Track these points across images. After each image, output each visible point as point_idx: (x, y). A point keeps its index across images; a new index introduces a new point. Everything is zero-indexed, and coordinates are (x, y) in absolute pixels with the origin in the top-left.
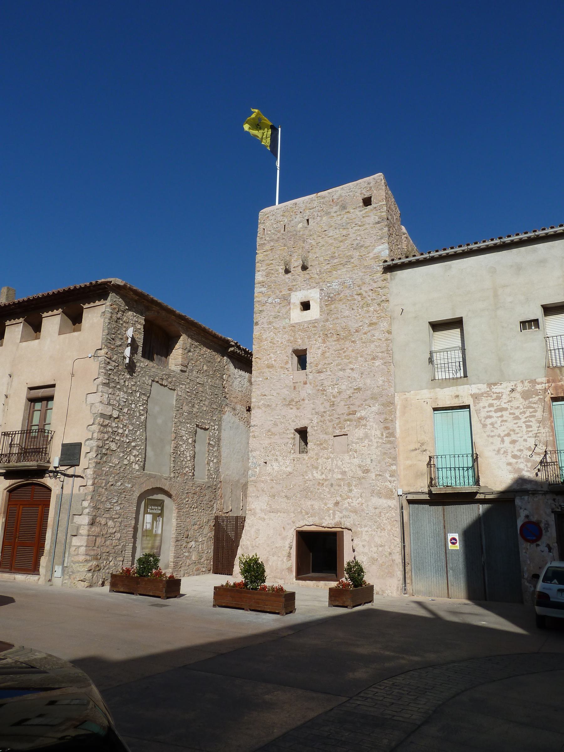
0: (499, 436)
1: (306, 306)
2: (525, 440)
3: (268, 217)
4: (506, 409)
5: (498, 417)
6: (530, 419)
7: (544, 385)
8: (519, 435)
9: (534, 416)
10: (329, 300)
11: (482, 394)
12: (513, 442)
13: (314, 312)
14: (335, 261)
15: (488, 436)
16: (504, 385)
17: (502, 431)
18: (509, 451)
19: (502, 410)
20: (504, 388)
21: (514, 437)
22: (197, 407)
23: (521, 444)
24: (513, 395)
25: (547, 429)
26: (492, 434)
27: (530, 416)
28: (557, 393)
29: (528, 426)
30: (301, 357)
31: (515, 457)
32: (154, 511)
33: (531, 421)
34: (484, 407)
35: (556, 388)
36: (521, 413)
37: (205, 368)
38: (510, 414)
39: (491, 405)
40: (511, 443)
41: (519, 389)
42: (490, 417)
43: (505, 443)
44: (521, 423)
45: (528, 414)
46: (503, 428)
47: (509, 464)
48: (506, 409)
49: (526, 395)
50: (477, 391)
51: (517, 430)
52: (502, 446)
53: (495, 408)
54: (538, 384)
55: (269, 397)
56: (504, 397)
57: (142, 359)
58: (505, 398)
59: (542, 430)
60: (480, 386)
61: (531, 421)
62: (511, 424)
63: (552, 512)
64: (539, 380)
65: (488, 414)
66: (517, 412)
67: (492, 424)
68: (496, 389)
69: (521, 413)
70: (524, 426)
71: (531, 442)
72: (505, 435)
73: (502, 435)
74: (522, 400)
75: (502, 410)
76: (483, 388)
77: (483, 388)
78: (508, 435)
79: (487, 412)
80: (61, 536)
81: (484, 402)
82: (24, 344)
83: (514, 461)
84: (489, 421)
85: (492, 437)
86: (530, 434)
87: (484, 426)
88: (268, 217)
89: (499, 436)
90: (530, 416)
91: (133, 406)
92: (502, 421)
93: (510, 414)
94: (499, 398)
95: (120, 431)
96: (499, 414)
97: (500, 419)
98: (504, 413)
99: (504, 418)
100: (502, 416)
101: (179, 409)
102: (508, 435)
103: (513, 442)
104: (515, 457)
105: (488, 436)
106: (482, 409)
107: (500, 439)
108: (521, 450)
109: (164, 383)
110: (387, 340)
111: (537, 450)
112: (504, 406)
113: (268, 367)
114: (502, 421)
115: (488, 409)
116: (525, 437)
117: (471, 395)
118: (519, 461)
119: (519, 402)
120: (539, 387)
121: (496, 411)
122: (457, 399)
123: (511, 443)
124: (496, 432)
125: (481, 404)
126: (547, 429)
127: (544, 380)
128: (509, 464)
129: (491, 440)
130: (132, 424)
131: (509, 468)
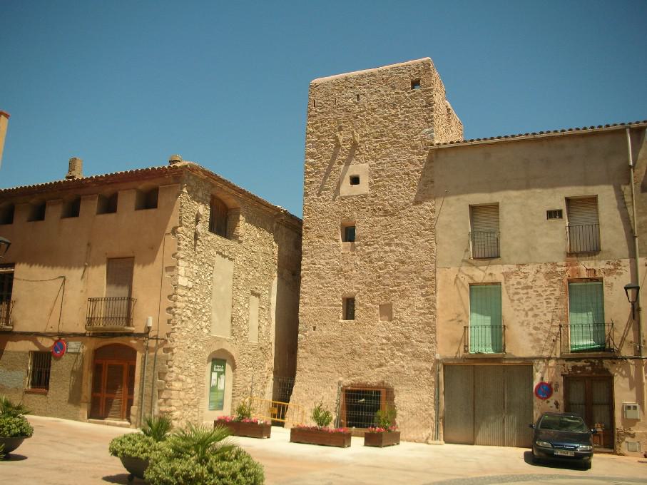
0: (524, 310)
1: (355, 180)
2: (545, 315)
3: (319, 89)
4: (531, 287)
5: (524, 294)
6: (551, 297)
7: (563, 268)
8: (540, 310)
9: (553, 294)
10: (375, 174)
11: (512, 273)
12: (536, 315)
13: (363, 188)
14: (384, 139)
15: (515, 310)
16: (530, 267)
17: (526, 306)
18: (532, 323)
19: (528, 287)
20: (530, 269)
21: (536, 311)
22: (252, 273)
23: (542, 318)
24: (538, 275)
25: (563, 306)
26: (518, 308)
27: (551, 294)
28: (573, 276)
29: (548, 303)
30: (349, 234)
31: (536, 328)
32: (219, 370)
33: (550, 299)
34: (513, 285)
35: (573, 271)
36: (543, 291)
37: (258, 236)
38: (534, 291)
39: (519, 283)
40: (533, 316)
41: (543, 270)
42: (517, 293)
43: (529, 316)
44: (542, 299)
45: (548, 293)
46: (528, 304)
47: (531, 334)
48: (531, 287)
49: (548, 275)
50: (508, 270)
51: (539, 305)
52: (527, 319)
53: (522, 286)
54: (559, 266)
55: (319, 266)
56: (530, 276)
57: (209, 233)
58: (531, 278)
59: (559, 307)
60: (511, 266)
61: (550, 299)
62: (534, 301)
63: (562, 375)
64: (559, 264)
65: (516, 291)
66: (540, 290)
67: (519, 300)
68: (524, 269)
69: (543, 291)
70: (544, 302)
71: (549, 317)
72: (530, 310)
73: (527, 309)
74: (544, 280)
75: (528, 287)
76: (514, 268)
77: (514, 268)
78: (532, 309)
79: (516, 289)
80: (147, 389)
81: (513, 280)
82: (101, 216)
83: (534, 332)
84: (516, 297)
85: (518, 310)
86: (549, 309)
87: (512, 301)
88: (319, 89)
89: (524, 310)
90: (551, 294)
91: (203, 276)
92: (528, 297)
93: (534, 291)
94: (526, 277)
95: (194, 300)
96: (525, 291)
97: (526, 296)
98: (529, 291)
99: (529, 295)
100: (527, 293)
101: (236, 277)
102: (532, 309)
103: (536, 315)
104: (536, 328)
105: (515, 310)
106: (511, 287)
107: (524, 313)
108: (541, 323)
109: (226, 254)
110: (431, 219)
111: (554, 324)
112: (530, 284)
113: (318, 237)
114: (528, 297)
115: (516, 286)
116: (545, 312)
117: (503, 273)
118: (539, 332)
119: (542, 281)
120: (559, 269)
121: (523, 289)
122: (490, 277)
123: (533, 316)
124: (522, 307)
125: (511, 282)
126: (563, 306)
127: (564, 263)
128: (531, 334)
129: (517, 313)
130: (202, 293)
131: (530, 337)
